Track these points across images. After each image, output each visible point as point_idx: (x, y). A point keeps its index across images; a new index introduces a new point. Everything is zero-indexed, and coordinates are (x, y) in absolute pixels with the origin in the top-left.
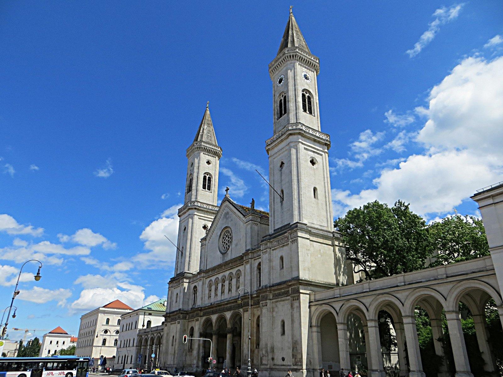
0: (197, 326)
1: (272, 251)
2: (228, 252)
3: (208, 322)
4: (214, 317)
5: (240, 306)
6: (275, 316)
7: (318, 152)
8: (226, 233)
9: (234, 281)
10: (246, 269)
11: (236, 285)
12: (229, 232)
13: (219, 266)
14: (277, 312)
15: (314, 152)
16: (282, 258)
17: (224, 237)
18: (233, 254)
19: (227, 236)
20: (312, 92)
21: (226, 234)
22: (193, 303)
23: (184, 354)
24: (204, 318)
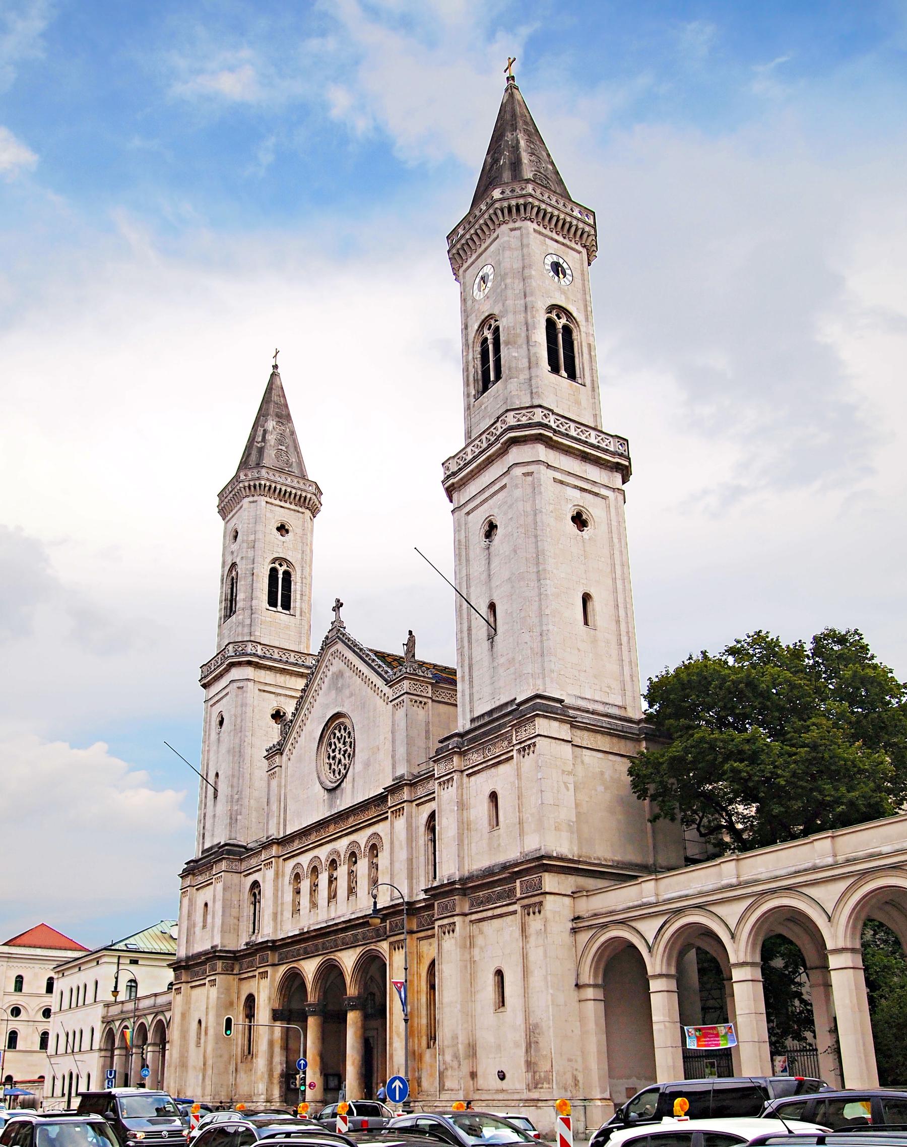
0: (265, 990)
1: (465, 779)
2: (344, 785)
5: (381, 935)
6: (476, 958)
7: (596, 490)
8: (337, 731)
9: (362, 866)
10: (395, 832)
11: (369, 875)
12: (345, 729)
14: (481, 948)
15: (583, 490)
16: (494, 796)
17: (333, 741)
19: (339, 739)
20: (575, 315)
21: (338, 734)
22: (251, 930)
23: (232, 1068)
24: (282, 969)
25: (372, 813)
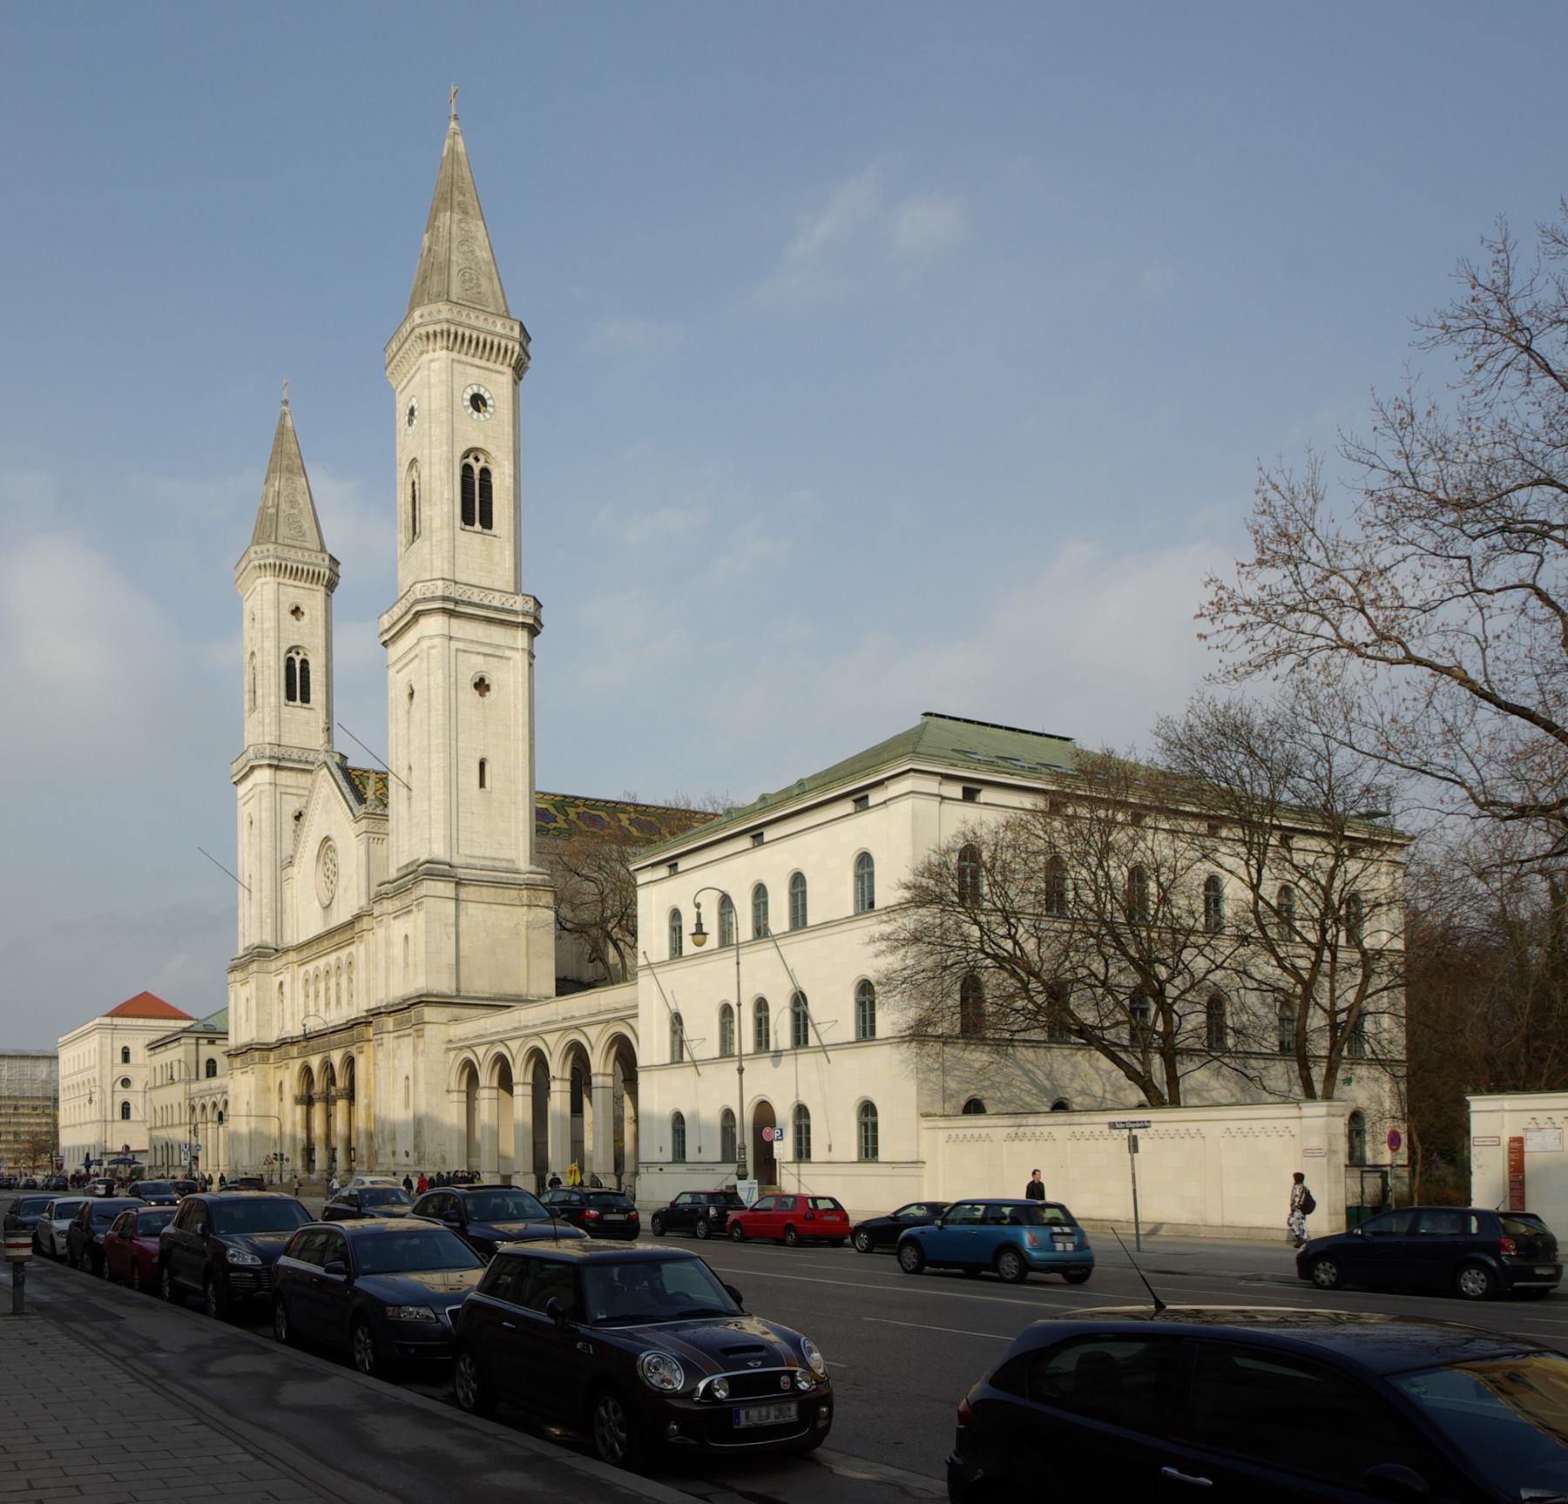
0: (290, 1077)
3: (307, 1070)
4: (315, 1062)
9: (344, 980)
13: (318, 939)
18: (341, 915)
24: (300, 1061)
25: (348, 935)
